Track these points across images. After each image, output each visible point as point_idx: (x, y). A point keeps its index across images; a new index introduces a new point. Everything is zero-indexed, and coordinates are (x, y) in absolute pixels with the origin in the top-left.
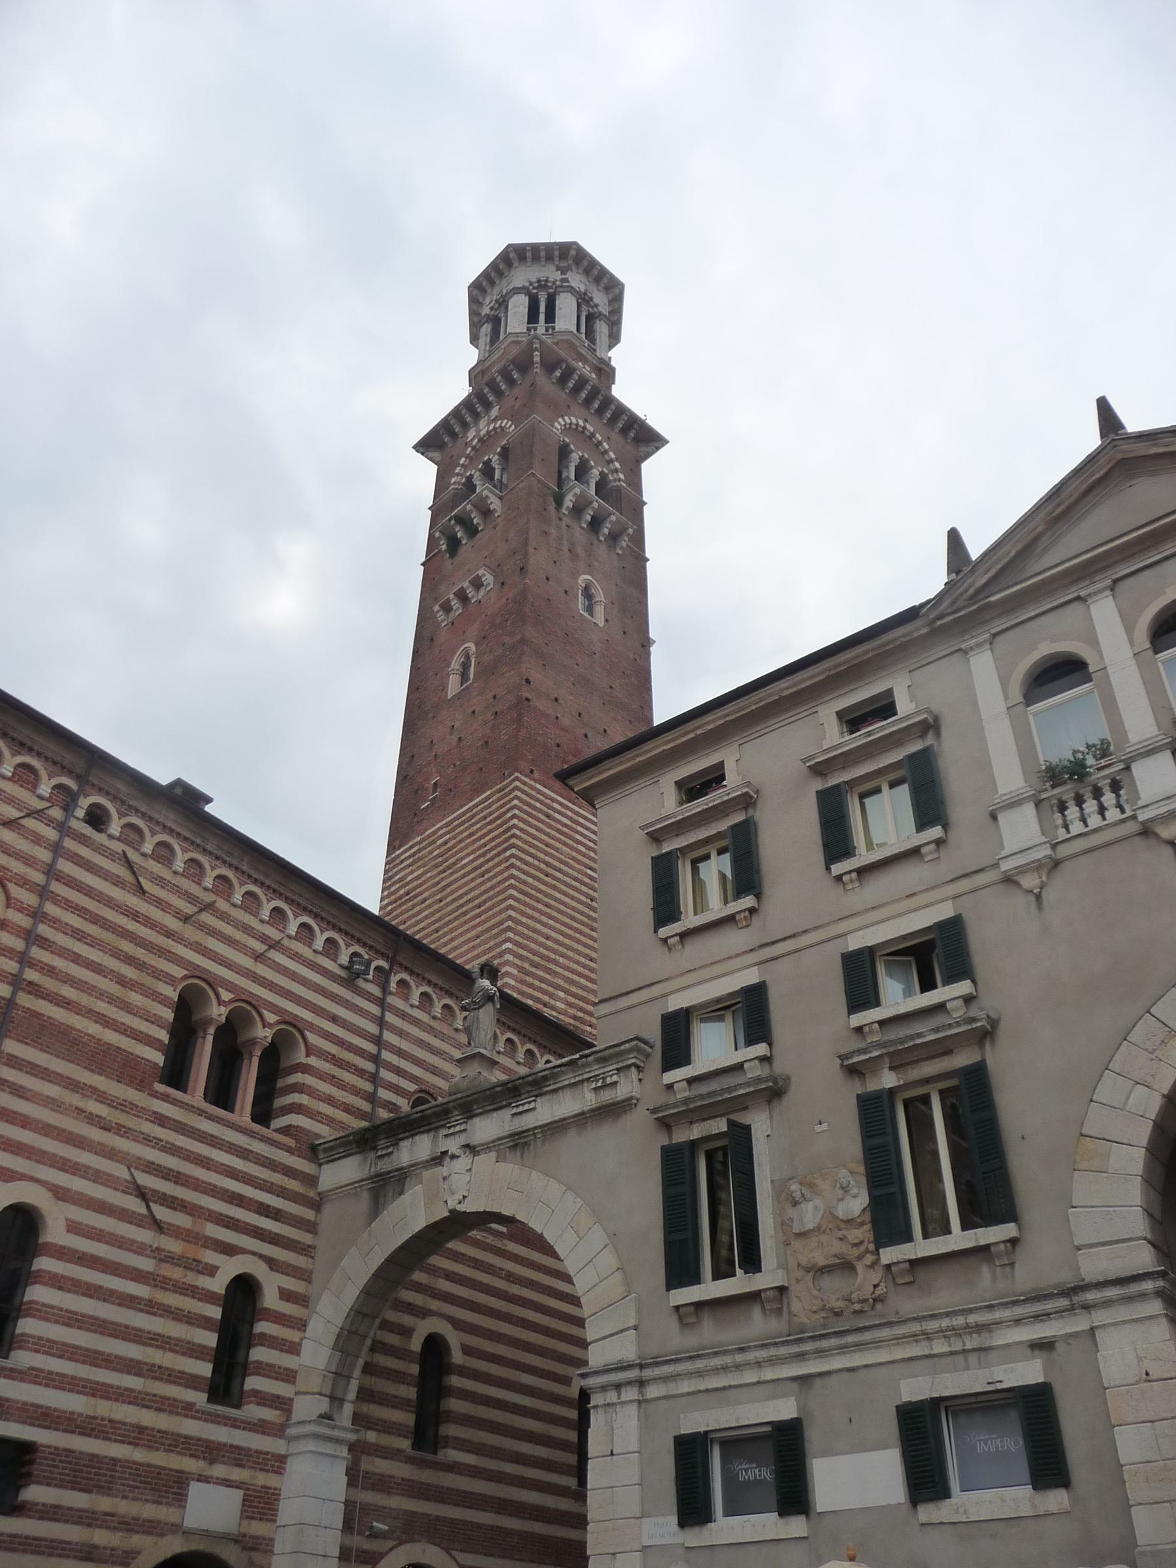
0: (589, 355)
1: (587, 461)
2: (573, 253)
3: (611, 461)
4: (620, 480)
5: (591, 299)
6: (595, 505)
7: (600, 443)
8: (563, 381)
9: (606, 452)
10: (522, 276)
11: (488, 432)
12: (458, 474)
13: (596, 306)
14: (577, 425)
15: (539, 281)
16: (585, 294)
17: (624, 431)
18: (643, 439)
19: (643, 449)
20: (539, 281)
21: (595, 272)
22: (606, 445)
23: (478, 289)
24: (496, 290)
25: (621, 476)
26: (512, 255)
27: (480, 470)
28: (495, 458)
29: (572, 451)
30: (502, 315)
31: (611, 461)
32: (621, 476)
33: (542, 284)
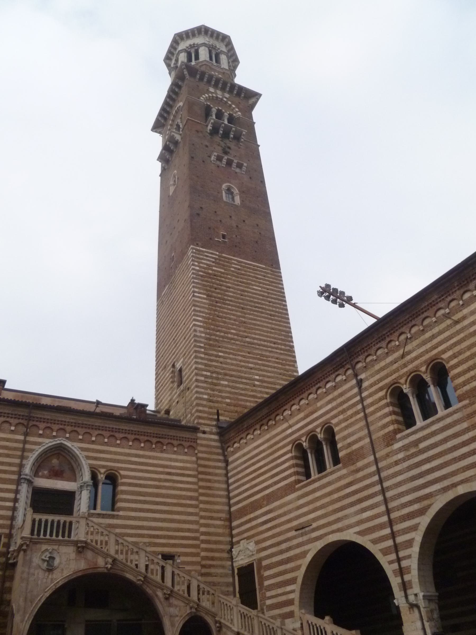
0: (218, 69)
2: (203, 30)
4: (239, 115)
5: (216, 47)
8: (201, 79)
10: (183, 46)
13: (219, 49)
14: (213, 97)
16: (212, 45)
17: (238, 94)
18: (249, 98)
19: (251, 101)
20: (190, 45)
21: (215, 35)
27: (175, 129)
29: (212, 108)
31: (234, 108)
33: (192, 46)
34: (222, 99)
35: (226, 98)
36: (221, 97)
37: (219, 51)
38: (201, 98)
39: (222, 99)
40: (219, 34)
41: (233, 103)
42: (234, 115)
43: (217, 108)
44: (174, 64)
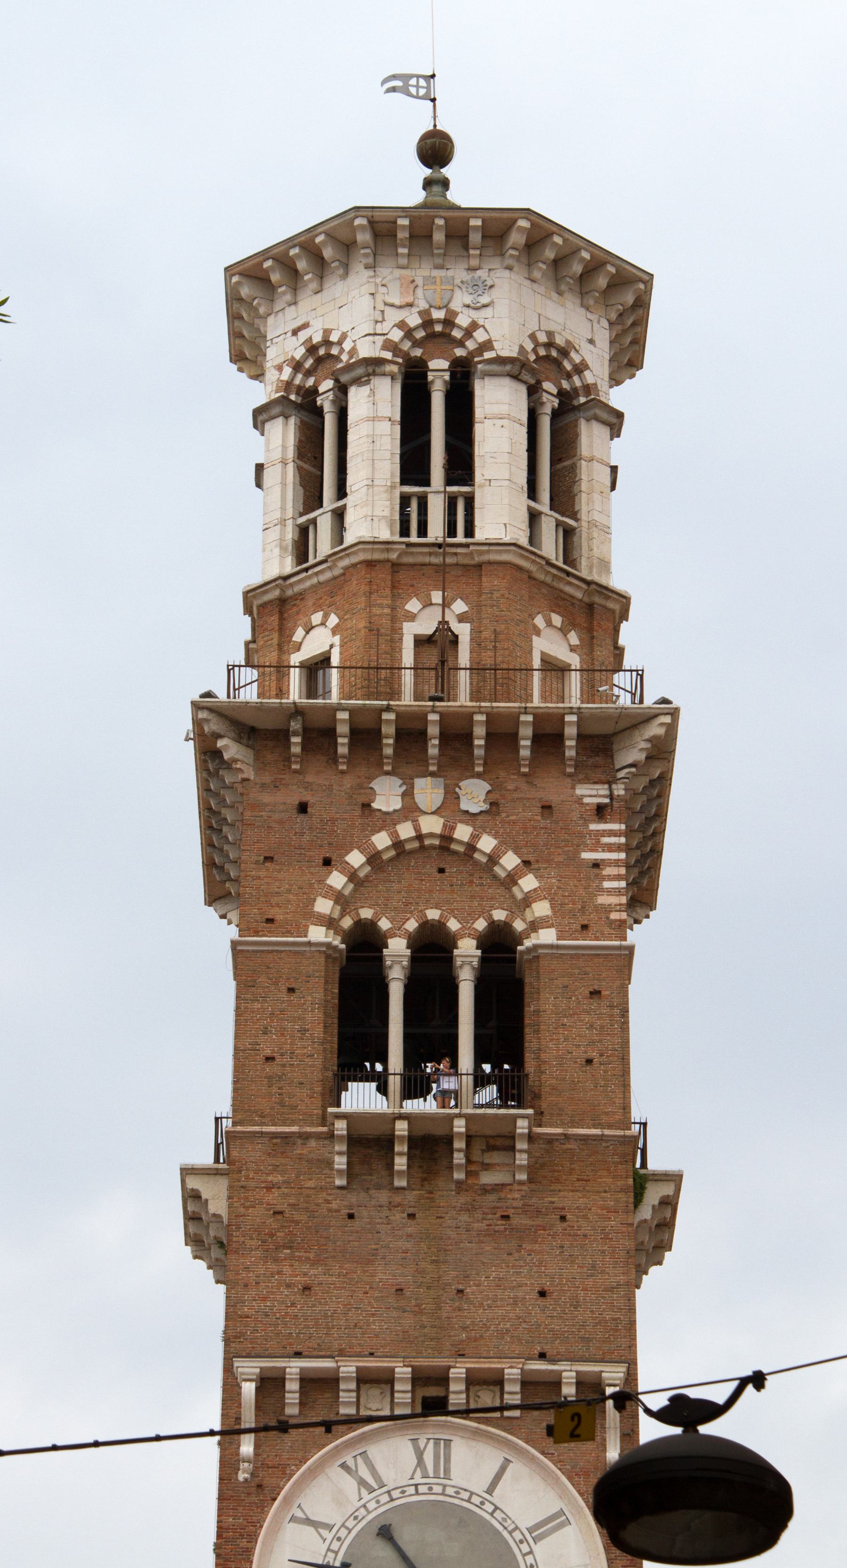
3: (512, 879)
7: (471, 847)
9: (493, 859)
31: (512, 879)
32: (541, 909)
34: (447, 838)
35: (469, 817)
38: (324, 906)
39: (447, 838)
41: (506, 843)
42: (519, 926)
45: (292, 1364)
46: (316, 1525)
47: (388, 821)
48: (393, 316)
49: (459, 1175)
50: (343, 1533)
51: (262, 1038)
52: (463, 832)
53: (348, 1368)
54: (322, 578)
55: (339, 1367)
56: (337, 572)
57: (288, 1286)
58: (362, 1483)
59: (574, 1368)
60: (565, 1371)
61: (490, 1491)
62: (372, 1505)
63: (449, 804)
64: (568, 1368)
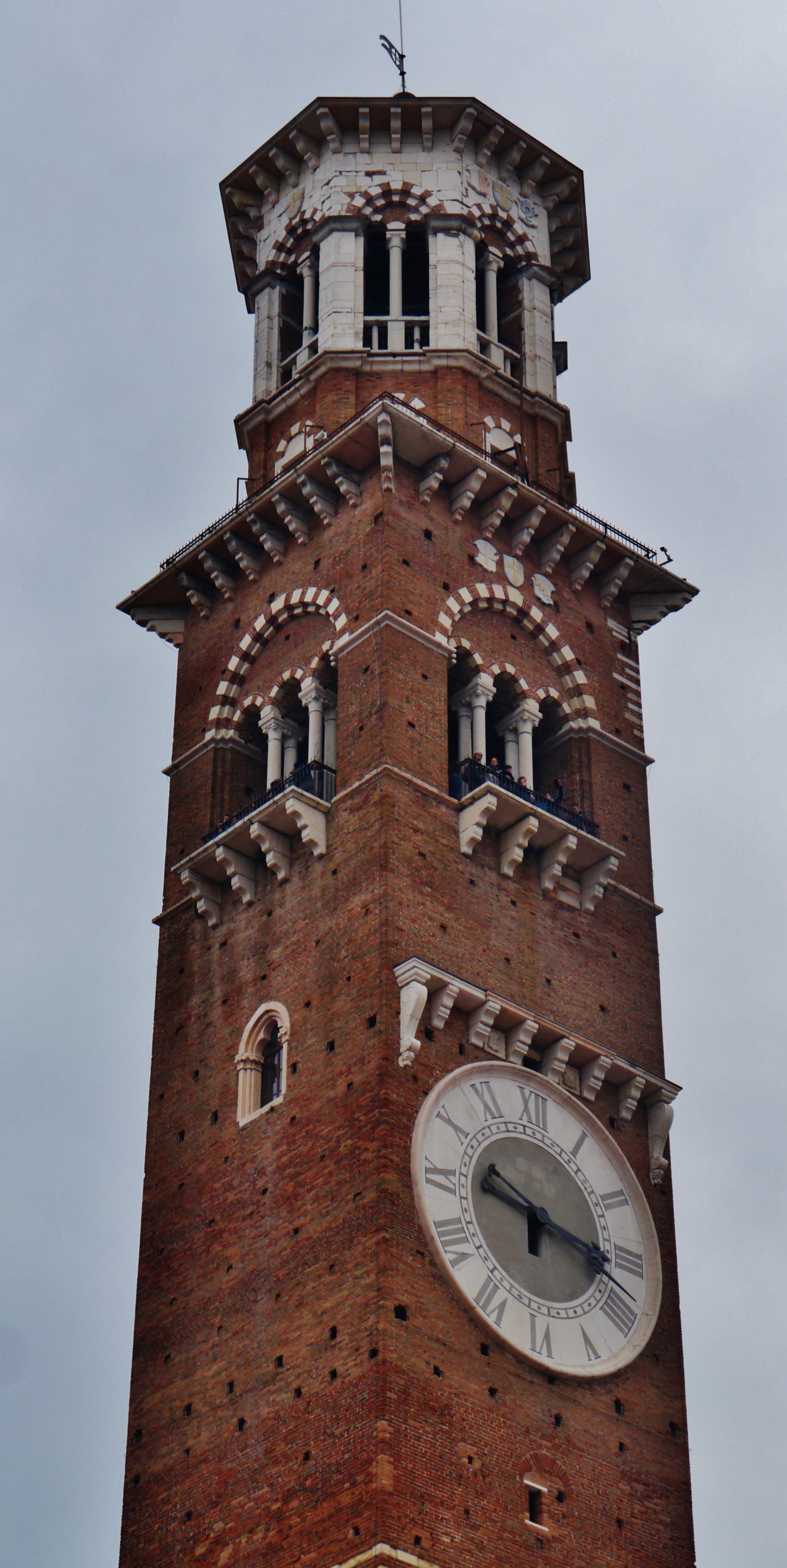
1: (514, 680)
3: (566, 669)
4: (584, 713)
5: (508, 224)
6: (533, 823)
7: (540, 629)
9: (554, 646)
11: (288, 607)
12: (226, 700)
13: (522, 239)
15: (387, 192)
16: (494, 217)
20: (387, 192)
22: (552, 631)
23: (246, 192)
24: (288, 198)
25: (589, 702)
26: (326, 124)
28: (308, 685)
29: (477, 670)
30: (306, 272)
31: (566, 669)
32: (589, 702)
33: (395, 201)
34: (523, 613)
35: (542, 605)
36: (517, 597)
37: (520, 250)
38: (445, 621)
40: (535, 150)
42: (565, 706)
43: (496, 670)
44: (280, 247)
45: (454, 983)
46: (457, 1128)
47: (484, 576)
48: (473, 199)
49: (549, 885)
50: (475, 1143)
51: (405, 705)
52: (536, 614)
53: (495, 1005)
54: (407, 368)
55: (487, 1001)
56: (426, 367)
57: (430, 918)
58: (487, 1107)
59: (646, 1076)
60: (639, 1076)
61: (575, 1152)
62: (494, 1129)
63: (527, 587)
64: (642, 1074)
